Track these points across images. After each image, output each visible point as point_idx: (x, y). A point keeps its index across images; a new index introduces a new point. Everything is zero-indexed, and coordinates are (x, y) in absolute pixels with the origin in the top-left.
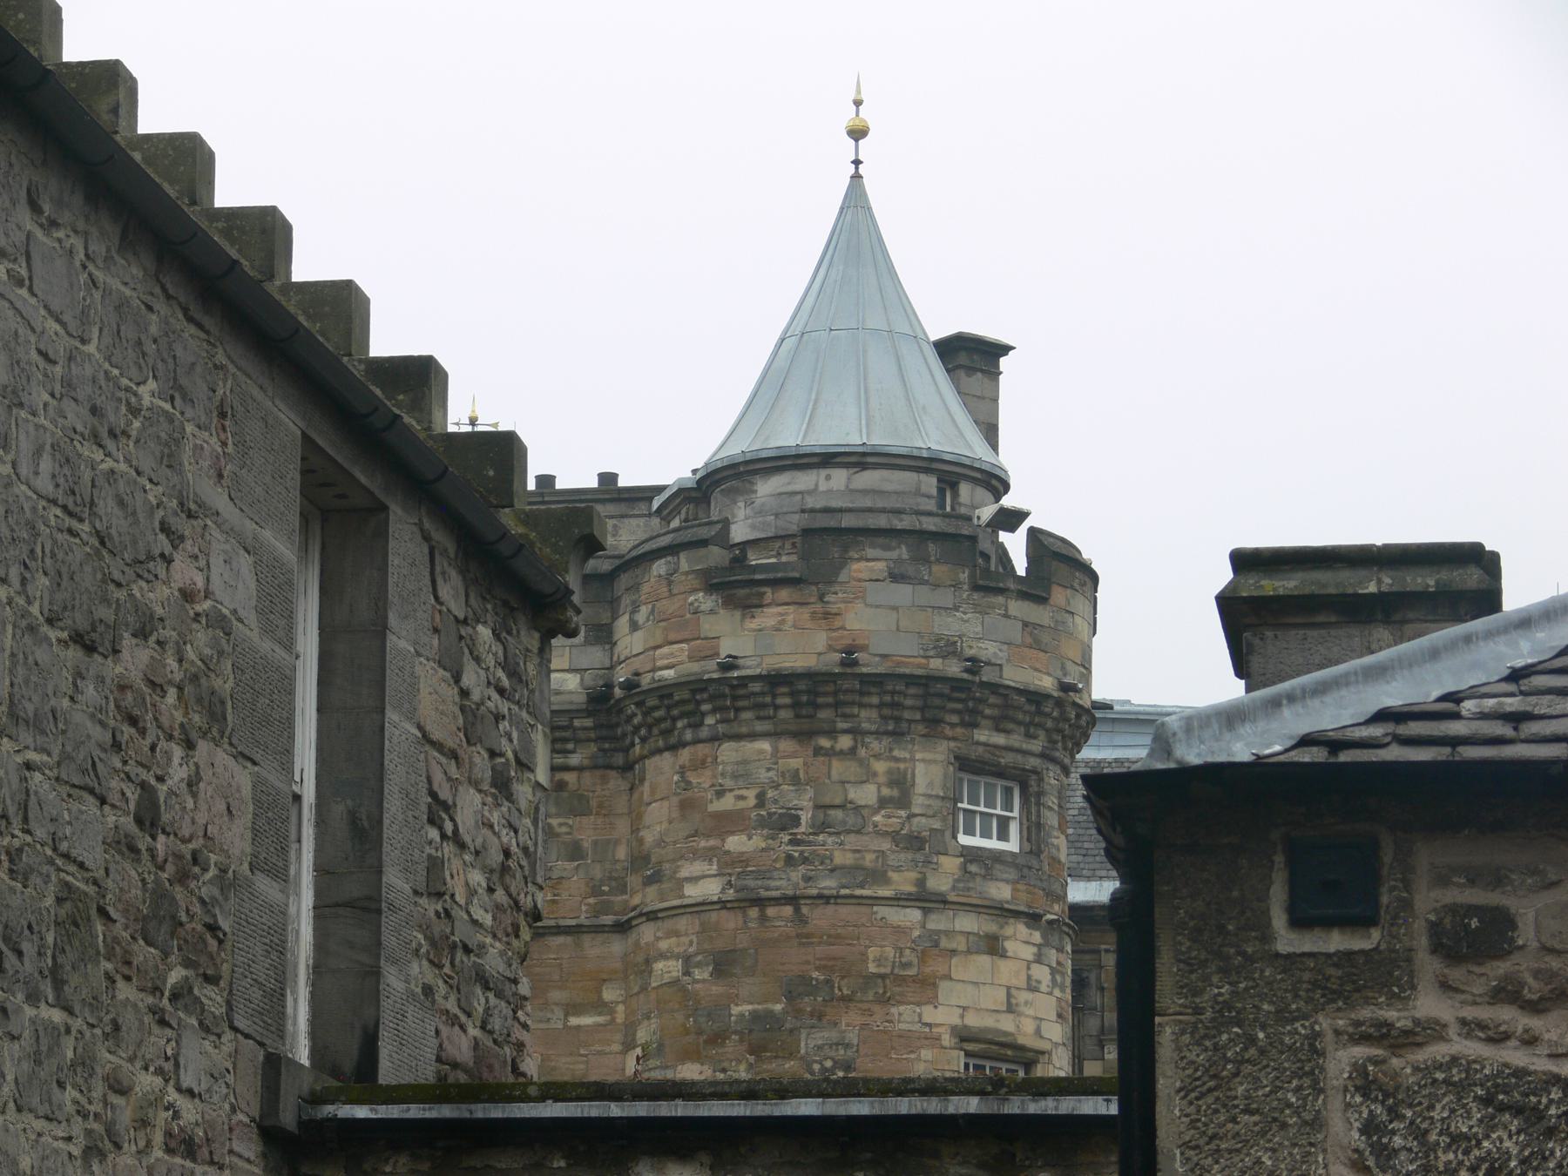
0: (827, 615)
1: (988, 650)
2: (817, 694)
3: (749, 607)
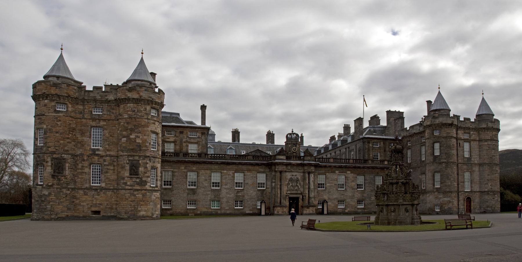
1: (154, 98)
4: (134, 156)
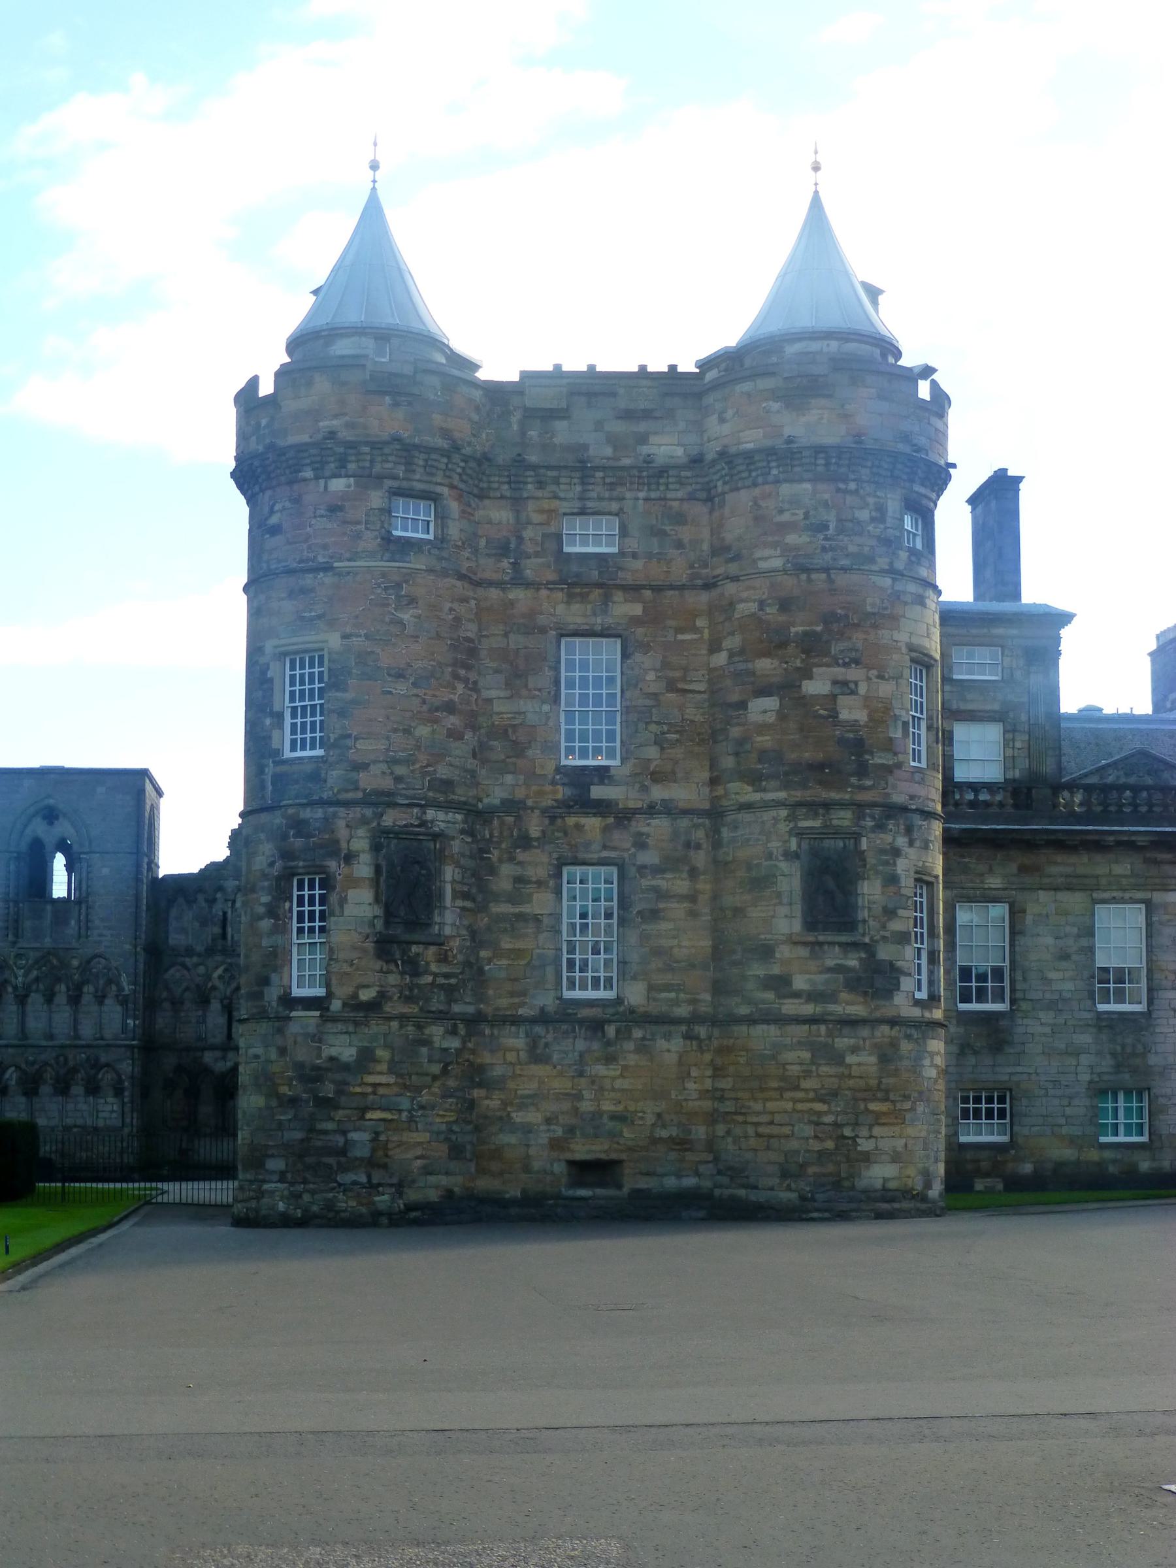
1: (922, 441)
4: (827, 806)
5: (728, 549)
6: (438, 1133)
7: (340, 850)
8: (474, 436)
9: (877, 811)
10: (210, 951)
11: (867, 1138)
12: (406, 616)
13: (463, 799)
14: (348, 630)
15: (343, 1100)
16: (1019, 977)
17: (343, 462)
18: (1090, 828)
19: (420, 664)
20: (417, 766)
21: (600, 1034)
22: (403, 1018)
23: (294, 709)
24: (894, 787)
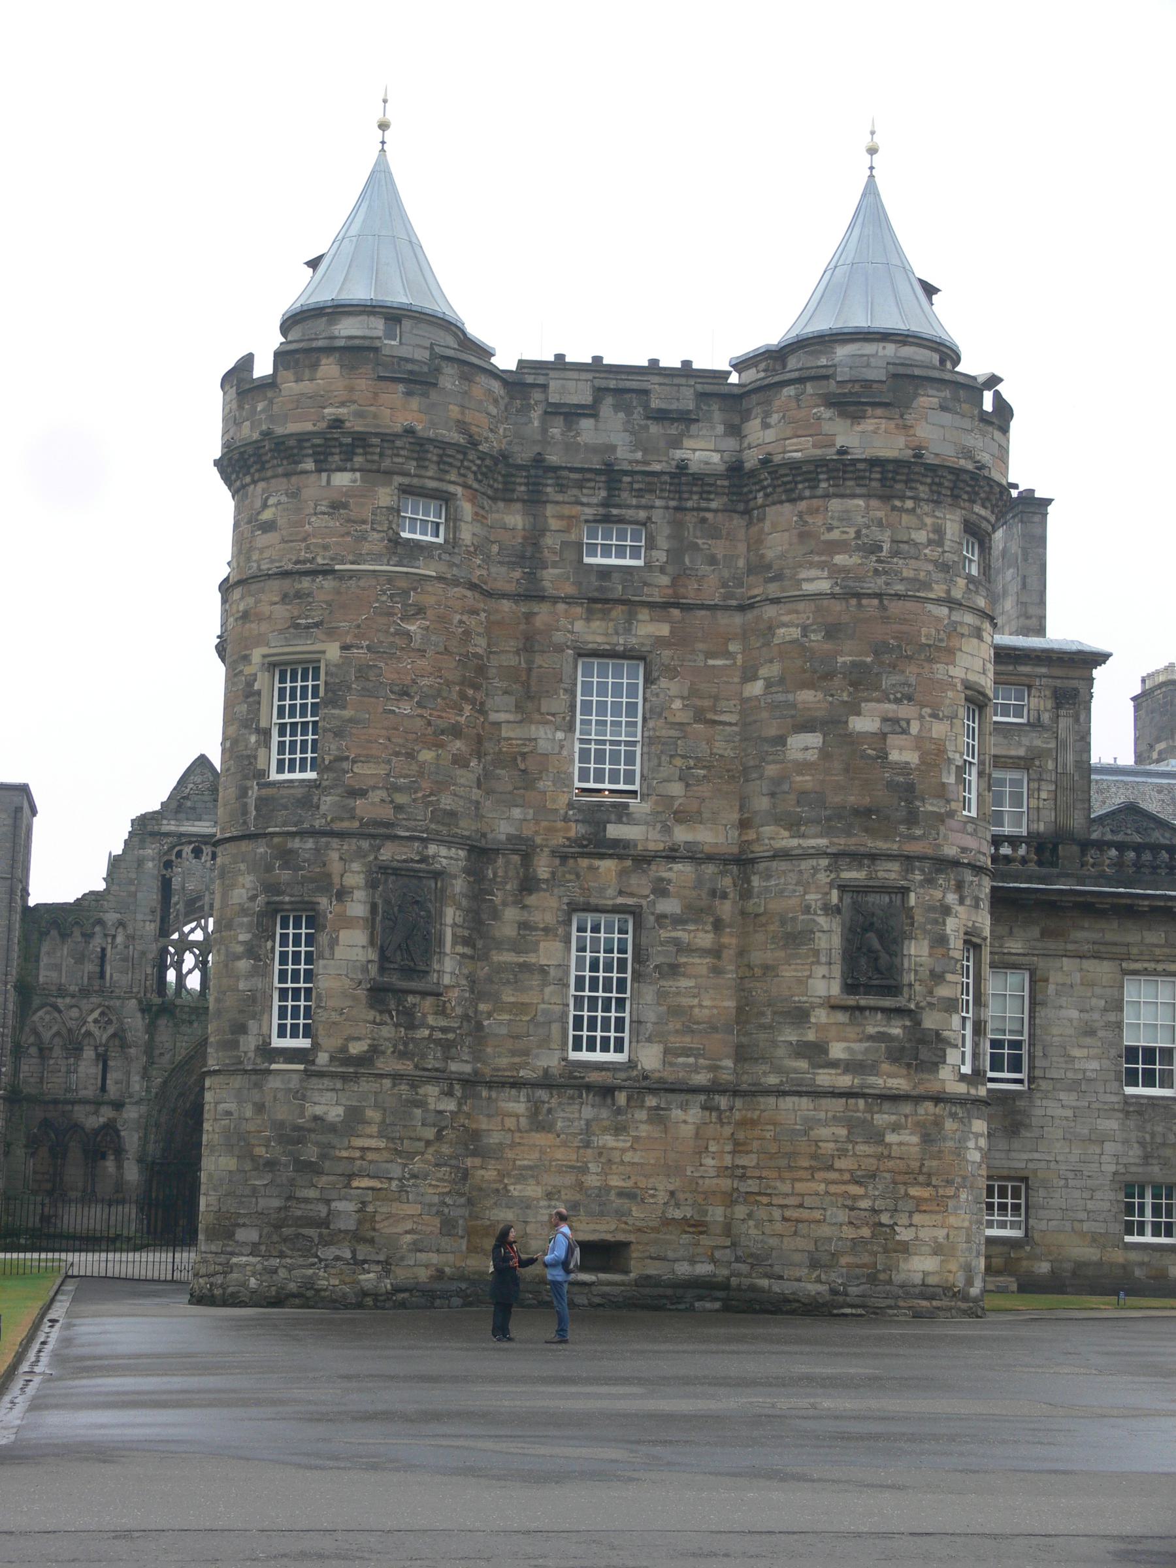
0: (905, 427)
1: (985, 458)
2: (898, 474)
3: (857, 418)
4: (873, 857)
5: (769, 567)
6: (431, 1205)
7: (331, 884)
8: (491, 430)
9: (927, 866)
10: (85, 992)
11: (906, 1227)
12: (412, 628)
13: (466, 833)
14: (349, 640)
15: (327, 1165)
16: (1039, 1053)
17: (349, 454)
18: (1121, 890)
19: (425, 682)
20: (420, 795)
21: (609, 1101)
22: (396, 1077)
23: (282, 728)
24: (946, 838)
